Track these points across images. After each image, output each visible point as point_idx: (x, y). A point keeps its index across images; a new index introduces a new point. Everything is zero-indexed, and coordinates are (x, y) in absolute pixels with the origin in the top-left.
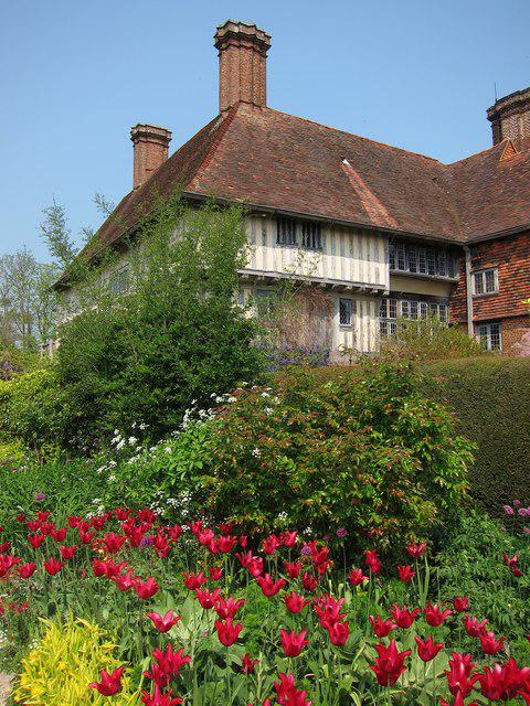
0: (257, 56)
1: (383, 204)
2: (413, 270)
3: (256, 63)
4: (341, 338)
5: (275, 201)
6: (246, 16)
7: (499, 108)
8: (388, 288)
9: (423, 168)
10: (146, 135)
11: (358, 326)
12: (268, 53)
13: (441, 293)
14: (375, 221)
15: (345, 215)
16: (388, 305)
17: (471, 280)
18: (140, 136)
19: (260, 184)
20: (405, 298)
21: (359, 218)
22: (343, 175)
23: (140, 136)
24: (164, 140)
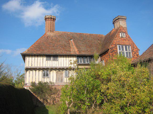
1: (77, 48)
14: (72, 53)
15: (64, 53)
21: (68, 53)
22: (69, 43)
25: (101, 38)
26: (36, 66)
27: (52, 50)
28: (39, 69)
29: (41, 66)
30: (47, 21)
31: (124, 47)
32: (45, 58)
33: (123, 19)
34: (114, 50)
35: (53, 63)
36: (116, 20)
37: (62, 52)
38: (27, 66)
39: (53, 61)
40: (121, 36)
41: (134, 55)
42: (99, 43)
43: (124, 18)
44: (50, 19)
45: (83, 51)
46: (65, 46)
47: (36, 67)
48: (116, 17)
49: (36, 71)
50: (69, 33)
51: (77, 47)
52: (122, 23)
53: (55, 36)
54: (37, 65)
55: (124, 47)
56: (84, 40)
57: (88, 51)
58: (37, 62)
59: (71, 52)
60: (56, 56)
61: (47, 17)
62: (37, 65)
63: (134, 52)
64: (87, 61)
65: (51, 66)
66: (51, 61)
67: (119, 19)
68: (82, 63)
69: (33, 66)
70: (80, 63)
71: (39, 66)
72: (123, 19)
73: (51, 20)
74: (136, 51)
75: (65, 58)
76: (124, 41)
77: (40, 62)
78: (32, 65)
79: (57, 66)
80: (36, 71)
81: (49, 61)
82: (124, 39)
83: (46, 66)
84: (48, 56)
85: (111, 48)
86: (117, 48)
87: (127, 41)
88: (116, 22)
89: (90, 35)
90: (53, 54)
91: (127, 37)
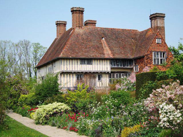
0: (80, 14)
1: (111, 50)
3: (80, 16)
4: (98, 84)
5: (81, 55)
6: (77, 5)
7: (151, 17)
8: (110, 71)
9: (132, 34)
10: (59, 24)
11: (103, 82)
12: (84, 12)
13: (128, 71)
15: (99, 56)
16: (112, 75)
17: (134, 68)
18: (58, 24)
19: (77, 51)
20: (117, 73)
21: (102, 56)
22: (101, 43)
23: (58, 24)
24: (65, 24)
25: (135, 34)
26: (71, 70)
27: (85, 52)
28: (75, 73)
29: (76, 70)
30: (75, 14)
31: (159, 53)
32: (79, 62)
34: (149, 57)
38: (63, 70)
39: (87, 65)
40: (157, 42)
41: (168, 61)
42: (133, 42)
44: (78, 12)
45: (117, 54)
46: (98, 47)
48: (153, 14)
50: (99, 29)
51: (111, 49)
52: (159, 22)
53: (85, 33)
55: (159, 53)
57: (122, 54)
59: (104, 55)
60: (89, 60)
61: (75, 9)
63: (168, 58)
66: (85, 65)
67: (157, 16)
69: (68, 70)
70: (113, 67)
71: (74, 70)
72: (161, 17)
74: (170, 57)
76: (160, 48)
81: (83, 65)
82: (160, 45)
85: (146, 55)
86: (152, 55)
87: (162, 48)
89: (122, 30)
91: (163, 43)
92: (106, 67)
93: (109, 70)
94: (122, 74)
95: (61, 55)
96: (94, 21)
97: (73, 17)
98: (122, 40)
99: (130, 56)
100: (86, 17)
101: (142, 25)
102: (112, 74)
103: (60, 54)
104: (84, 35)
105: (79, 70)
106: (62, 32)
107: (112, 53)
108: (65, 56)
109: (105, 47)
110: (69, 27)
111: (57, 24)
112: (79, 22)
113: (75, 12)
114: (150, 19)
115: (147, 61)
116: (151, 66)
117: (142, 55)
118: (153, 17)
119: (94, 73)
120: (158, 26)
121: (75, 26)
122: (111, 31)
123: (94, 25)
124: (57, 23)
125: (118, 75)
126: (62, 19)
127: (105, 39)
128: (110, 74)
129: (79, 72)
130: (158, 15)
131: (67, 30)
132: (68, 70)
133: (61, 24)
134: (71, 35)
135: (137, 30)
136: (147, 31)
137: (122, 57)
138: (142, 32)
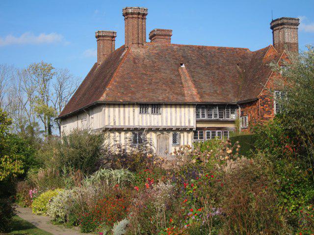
2: (210, 115)
3: (140, 23)
5: (140, 97)
7: (272, 25)
8: (195, 127)
12: (147, 17)
14: (188, 99)
15: (173, 98)
16: (198, 134)
19: (133, 89)
20: (208, 130)
21: (180, 99)
22: (179, 75)
25: (244, 57)
26: (122, 124)
27: (149, 92)
29: (132, 124)
30: (131, 20)
32: (137, 110)
33: (292, 24)
34: (267, 101)
35: (152, 118)
36: (278, 25)
37: (168, 98)
38: (107, 124)
42: (239, 73)
43: (294, 22)
44: (136, 16)
45: (208, 95)
46: (173, 83)
47: (122, 127)
48: (277, 20)
49: (120, 133)
50: (175, 47)
52: (287, 35)
53: (149, 56)
54: (125, 122)
56: (208, 64)
57: (217, 93)
58: (124, 117)
60: (156, 106)
61: (130, 11)
62: (125, 122)
64: (216, 115)
65: (148, 125)
66: (148, 116)
67: (282, 24)
68: (206, 118)
69: (117, 124)
70: (201, 118)
71: (127, 124)
72: (292, 24)
73: (139, 18)
75: (173, 109)
77: (129, 117)
78: (115, 123)
79: (160, 125)
80: (120, 133)
81: (144, 115)
83: (141, 125)
84: (143, 106)
85: (261, 97)
88: (278, 29)
90: (152, 102)
92: (186, 117)
93: (193, 124)
94: (217, 131)
95: (103, 98)
96: (168, 31)
97: (127, 26)
98: (217, 69)
99: (232, 98)
100: (151, 25)
101: (255, 39)
102: (199, 131)
103: (101, 95)
104: (148, 59)
105: (136, 124)
106: (107, 52)
107: (198, 93)
108: (110, 99)
109: (186, 81)
110: (119, 43)
111: (98, 37)
112: (136, 36)
113: (131, 16)
114: (272, 28)
115: (263, 109)
116: (270, 118)
117: (254, 97)
118: (276, 25)
119: (164, 130)
120: (287, 41)
121: (131, 43)
122: (198, 52)
123: (167, 37)
124: (97, 34)
125: (211, 134)
126: (107, 28)
127: (185, 66)
128: (195, 132)
129: (136, 129)
130: (285, 21)
131: (117, 48)
132: (117, 124)
133: (103, 36)
134: (122, 59)
135: (246, 50)
136: (265, 51)
137: (217, 101)
138: (257, 53)
